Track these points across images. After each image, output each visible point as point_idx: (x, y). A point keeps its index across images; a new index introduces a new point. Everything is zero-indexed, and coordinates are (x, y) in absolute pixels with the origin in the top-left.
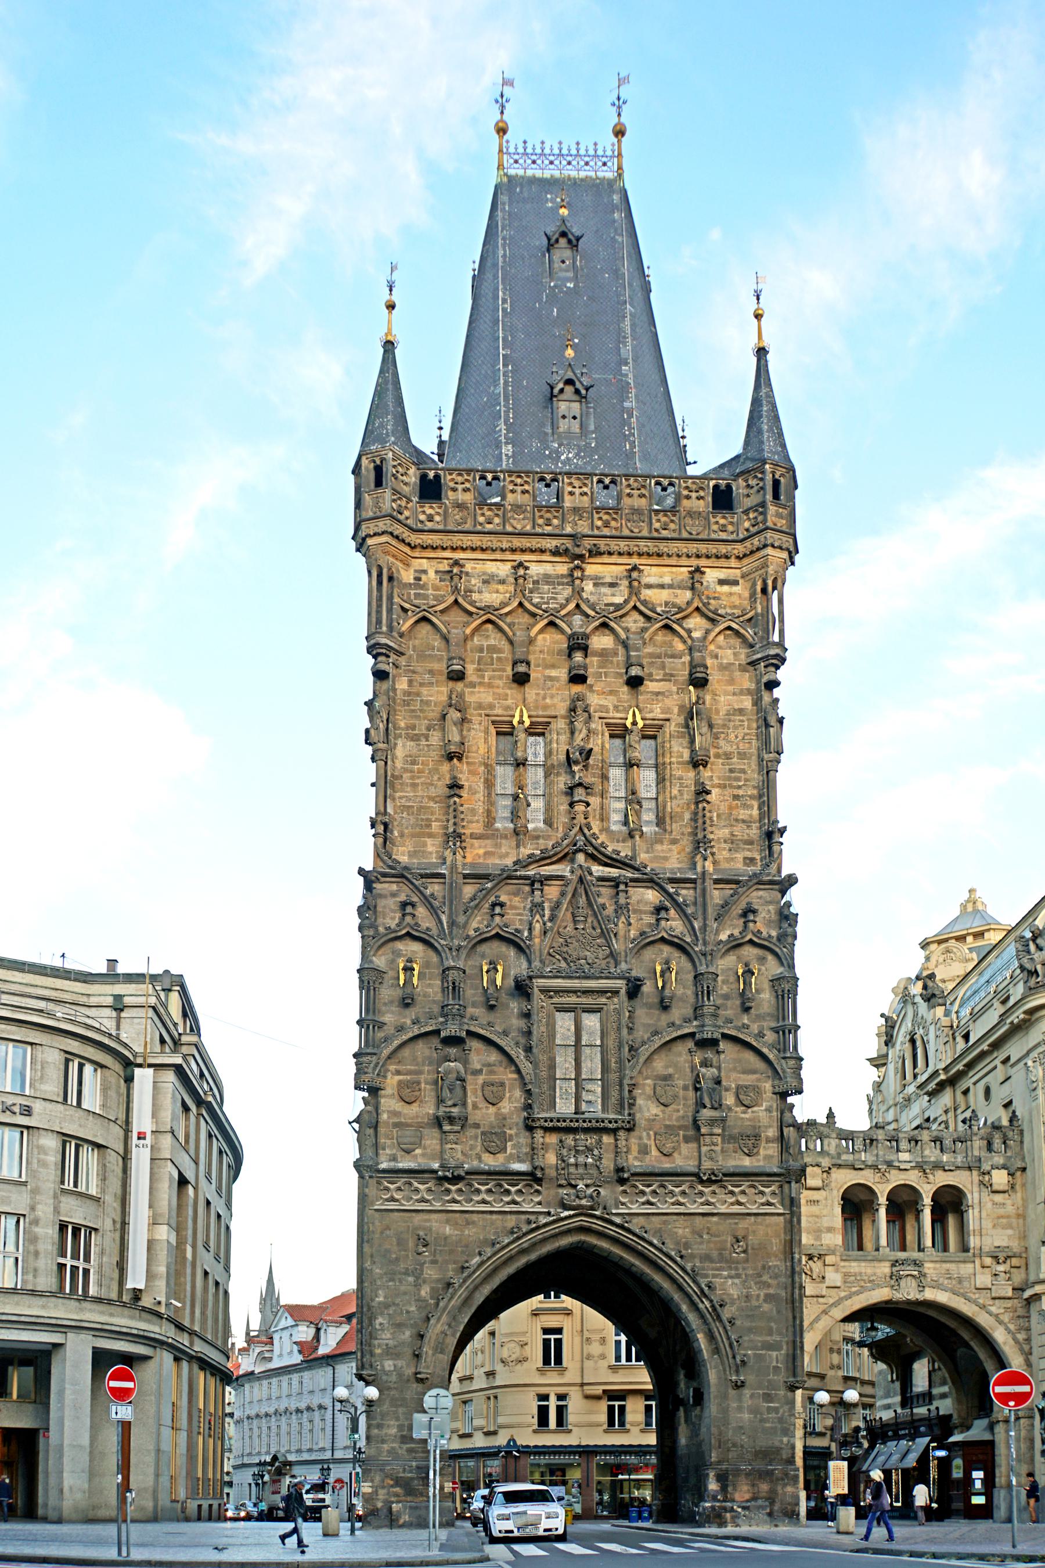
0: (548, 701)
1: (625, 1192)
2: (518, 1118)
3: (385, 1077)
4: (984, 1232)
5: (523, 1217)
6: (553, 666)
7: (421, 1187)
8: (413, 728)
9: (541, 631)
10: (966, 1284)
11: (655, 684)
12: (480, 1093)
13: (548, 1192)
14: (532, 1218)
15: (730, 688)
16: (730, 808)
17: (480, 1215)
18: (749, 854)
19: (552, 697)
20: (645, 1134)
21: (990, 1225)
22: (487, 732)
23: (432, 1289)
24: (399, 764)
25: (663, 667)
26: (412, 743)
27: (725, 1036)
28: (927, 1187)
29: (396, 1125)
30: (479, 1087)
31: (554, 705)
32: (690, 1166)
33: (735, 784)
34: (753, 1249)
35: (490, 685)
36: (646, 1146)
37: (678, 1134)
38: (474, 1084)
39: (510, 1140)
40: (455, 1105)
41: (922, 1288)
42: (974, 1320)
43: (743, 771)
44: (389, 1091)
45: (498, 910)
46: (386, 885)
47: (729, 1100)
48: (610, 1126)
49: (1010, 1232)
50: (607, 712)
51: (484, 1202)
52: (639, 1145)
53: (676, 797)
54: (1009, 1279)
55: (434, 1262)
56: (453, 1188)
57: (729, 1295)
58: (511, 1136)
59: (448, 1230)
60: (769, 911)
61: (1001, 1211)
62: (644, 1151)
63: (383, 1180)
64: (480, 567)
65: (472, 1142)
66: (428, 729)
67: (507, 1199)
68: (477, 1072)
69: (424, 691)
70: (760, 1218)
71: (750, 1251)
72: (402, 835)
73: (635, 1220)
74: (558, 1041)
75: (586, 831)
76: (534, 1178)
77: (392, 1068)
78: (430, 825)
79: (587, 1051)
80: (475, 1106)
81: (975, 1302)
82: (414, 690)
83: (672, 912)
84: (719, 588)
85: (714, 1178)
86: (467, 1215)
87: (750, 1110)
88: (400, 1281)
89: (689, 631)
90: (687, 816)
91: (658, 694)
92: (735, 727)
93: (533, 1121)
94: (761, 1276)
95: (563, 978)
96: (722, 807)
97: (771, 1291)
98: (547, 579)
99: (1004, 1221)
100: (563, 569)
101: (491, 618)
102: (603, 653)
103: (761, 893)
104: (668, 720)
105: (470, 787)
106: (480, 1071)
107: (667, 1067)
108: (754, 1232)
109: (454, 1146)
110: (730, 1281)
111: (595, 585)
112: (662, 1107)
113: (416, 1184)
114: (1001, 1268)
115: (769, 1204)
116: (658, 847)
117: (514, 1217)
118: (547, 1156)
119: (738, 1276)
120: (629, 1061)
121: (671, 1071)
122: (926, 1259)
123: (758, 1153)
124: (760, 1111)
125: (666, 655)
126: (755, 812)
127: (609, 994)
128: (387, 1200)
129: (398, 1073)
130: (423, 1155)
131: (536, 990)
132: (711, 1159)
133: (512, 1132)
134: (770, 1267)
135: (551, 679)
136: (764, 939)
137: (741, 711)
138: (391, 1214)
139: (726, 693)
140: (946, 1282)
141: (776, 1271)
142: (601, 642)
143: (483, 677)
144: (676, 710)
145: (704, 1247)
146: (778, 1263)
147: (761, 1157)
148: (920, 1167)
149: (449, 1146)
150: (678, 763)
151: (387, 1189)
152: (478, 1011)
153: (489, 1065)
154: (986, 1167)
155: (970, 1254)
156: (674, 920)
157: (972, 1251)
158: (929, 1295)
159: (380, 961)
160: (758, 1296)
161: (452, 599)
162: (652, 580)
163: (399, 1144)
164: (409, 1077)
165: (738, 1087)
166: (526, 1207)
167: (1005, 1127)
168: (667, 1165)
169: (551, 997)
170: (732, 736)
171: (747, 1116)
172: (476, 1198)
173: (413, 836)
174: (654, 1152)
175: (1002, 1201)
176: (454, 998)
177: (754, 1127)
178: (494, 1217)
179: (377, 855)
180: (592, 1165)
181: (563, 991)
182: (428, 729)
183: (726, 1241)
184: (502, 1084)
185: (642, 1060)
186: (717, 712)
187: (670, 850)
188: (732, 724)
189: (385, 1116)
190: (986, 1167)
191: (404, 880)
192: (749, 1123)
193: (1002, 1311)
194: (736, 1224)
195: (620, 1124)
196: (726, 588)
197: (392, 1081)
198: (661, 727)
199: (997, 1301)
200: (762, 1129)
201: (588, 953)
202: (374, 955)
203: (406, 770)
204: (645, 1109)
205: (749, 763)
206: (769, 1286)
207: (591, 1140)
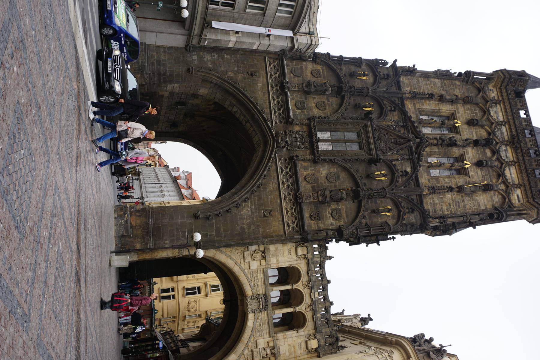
0: (465, 133)
1: (285, 160)
2: (311, 114)
3: (320, 65)
4: (286, 340)
5: (269, 116)
6: (476, 135)
7: (277, 75)
8: (445, 85)
9: (486, 130)
10: (258, 334)
11: (480, 172)
12: (320, 100)
13: (281, 126)
14: (270, 118)
15: (486, 201)
16: (446, 203)
17: (268, 98)
18: (431, 211)
19: (467, 134)
20: (313, 168)
21: (290, 343)
22: (450, 110)
23: (232, 77)
24: (432, 79)
25: (486, 175)
26: (440, 85)
27: (360, 203)
28: (304, 308)
29: (302, 68)
30: (322, 100)
31: (464, 135)
32: (302, 189)
33: (454, 204)
34: (266, 220)
35: (465, 113)
36: (308, 169)
37: (314, 184)
38: (323, 99)
39: (302, 112)
40: (315, 87)
41: (254, 311)
42: (239, 342)
43: (459, 207)
44: (315, 66)
45: (393, 108)
46: (391, 70)
47: (333, 206)
48: (316, 151)
49: (288, 354)
50: (467, 154)
51: (274, 100)
52: (308, 166)
53: (444, 181)
54: (263, 357)
55: (245, 78)
56: (278, 88)
57: (243, 209)
58: (304, 112)
59: (260, 85)
60: (412, 220)
61: (297, 348)
62: (306, 168)
63: (278, 60)
64: (499, 110)
65: (299, 96)
66: (446, 90)
67: (276, 109)
68: (328, 100)
69: (458, 90)
70: (281, 223)
71: (265, 218)
72: (409, 79)
73: (274, 165)
74: (345, 133)
75: (427, 143)
76: (287, 120)
77: (324, 68)
78: (414, 89)
79: (344, 145)
80: (314, 98)
81: (249, 340)
82: (457, 87)
83: (405, 178)
84: (516, 195)
85: (298, 199)
86: (267, 93)
87: (330, 215)
88: (234, 65)
89: (501, 184)
90: (439, 185)
91: (477, 173)
92: (473, 203)
93: (313, 118)
94: (253, 225)
95: (373, 132)
96: (445, 199)
97: (246, 230)
98: (502, 133)
99: (293, 350)
100: (506, 139)
101: (485, 112)
102: (485, 153)
103: (419, 216)
104: (469, 177)
105: (431, 104)
106: (329, 101)
107: (343, 178)
108: (275, 220)
109: (297, 88)
110: (249, 210)
111: (505, 150)
112: (325, 176)
113: (278, 73)
114: (269, 352)
115: (289, 226)
116: (426, 174)
117: (269, 112)
118: (298, 126)
119: (252, 213)
120: (344, 160)
121: (342, 179)
122: (269, 312)
123: (312, 220)
124: (331, 220)
125: (490, 176)
126: (446, 213)
127: (369, 152)
128: (270, 62)
129: (323, 70)
130: (291, 77)
131: (365, 122)
132: (307, 197)
133: (306, 113)
134: (258, 229)
135: (472, 134)
136: (403, 217)
137: (479, 205)
138: (264, 63)
139: (484, 199)
140: (258, 324)
141: (257, 232)
142: (489, 153)
143: (467, 110)
144: (474, 180)
145: (265, 197)
146: (261, 233)
147: (310, 222)
148: (313, 303)
149: (297, 86)
150: (456, 181)
151: (274, 62)
152: (352, 101)
153: (332, 104)
154: (318, 336)
155: (274, 335)
156: (402, 179)
157: (275, 335)
158: (251, 316)
159: (364, 66)
160: (243, 224)
161: (489, 100)
162: (512, 171)
163: (294, 68)
164: (322, 74)
165: (340, 210)
166: (274, 118)
167: (338, 344)
168: (300, 179)
169: (363, 129)
170: (470, 202)
171: (328, 214)
172: (275, 97)
173: (410, 83)
174: (305, 173)
175: (302, 348)
176: (357, 89)
177: (323, 218)
178: (268, 104)
179: (401, 67)
180: (297, 145)
181: (367, 133)
182: (446, 90)
183: (269, 207)
184: (325, 109)
185: (346, 166)
186: (477, 196)
187: (426, 179)
188: (474, 202)
189: (305, 64)
190: (318, 336)
191: (395, 77)
192: (324, 215)
193: (246, 357)
194: (278, 212)
195: (317, 155)
196: (516, 198)
197: (319, 67)
198: (466, 175)
199: (250, 353)
200: (323, 222)
201: (383, 143)
202: (366, 63)
203: (431, 82)
204: (324, 168)
205: (462, 209)
206: (249, 229)
207: (307, 145)
